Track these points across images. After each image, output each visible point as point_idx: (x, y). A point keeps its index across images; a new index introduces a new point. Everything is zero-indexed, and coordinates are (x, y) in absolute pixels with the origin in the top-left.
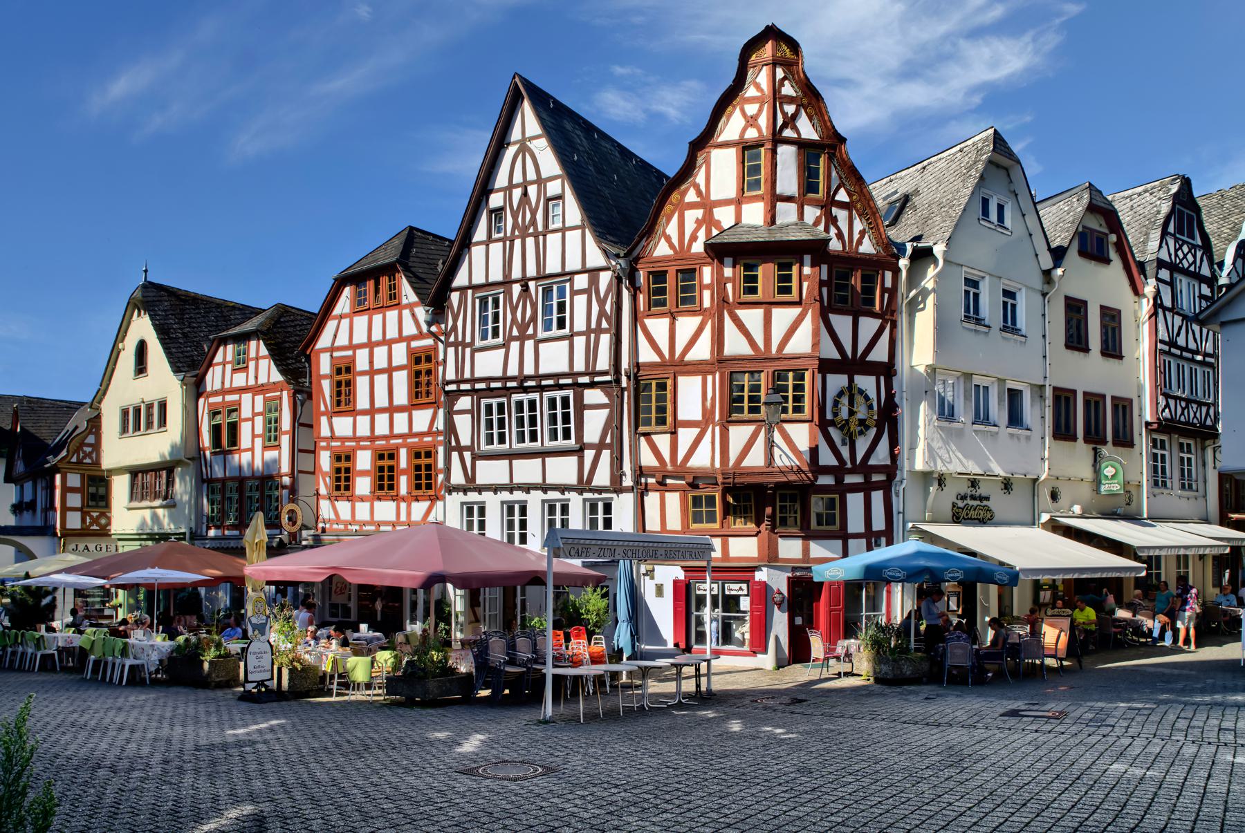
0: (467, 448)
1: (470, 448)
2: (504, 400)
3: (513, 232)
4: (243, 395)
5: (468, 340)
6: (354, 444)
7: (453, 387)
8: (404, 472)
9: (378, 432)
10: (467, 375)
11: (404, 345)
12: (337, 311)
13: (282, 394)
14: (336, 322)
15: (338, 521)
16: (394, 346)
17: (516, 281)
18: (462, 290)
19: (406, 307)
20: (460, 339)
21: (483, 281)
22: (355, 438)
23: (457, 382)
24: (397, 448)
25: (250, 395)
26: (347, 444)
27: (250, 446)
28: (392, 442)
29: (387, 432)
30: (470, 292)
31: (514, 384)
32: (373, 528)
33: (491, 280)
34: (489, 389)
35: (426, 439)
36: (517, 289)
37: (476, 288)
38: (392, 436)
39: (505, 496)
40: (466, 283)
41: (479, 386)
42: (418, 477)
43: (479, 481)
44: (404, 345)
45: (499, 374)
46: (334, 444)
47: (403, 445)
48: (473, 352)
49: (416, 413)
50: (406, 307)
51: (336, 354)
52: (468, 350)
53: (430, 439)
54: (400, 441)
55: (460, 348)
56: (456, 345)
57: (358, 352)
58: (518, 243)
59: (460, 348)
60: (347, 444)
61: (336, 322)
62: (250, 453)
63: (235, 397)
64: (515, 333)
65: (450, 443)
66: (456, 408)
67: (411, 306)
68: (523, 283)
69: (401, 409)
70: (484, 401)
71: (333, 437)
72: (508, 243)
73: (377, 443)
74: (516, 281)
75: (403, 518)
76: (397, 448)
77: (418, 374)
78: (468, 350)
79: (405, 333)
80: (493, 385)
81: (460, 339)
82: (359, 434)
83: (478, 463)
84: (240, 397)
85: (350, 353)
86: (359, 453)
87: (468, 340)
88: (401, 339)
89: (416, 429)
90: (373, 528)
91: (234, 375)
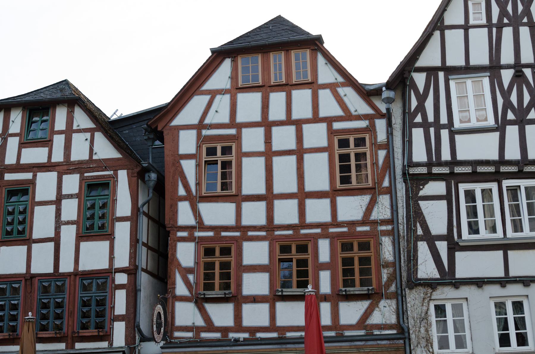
0: (440, 238)
1: (448, 237)
2: (494, 186)
3: (500, 19)
4: (39, 175)
5: (444, 120)
6: (237, 234)
7: (423, 170)
8: (324, 266)
9: (278, 221)
10: (446, 156)
11: (323, 126)
12: (207, 86)
13: (116, 175)
14: (207, 98)
15: (210, 326)
16: (306, 127)
17: (508, 67)
18: (431, 71)
19: (324, 86)
20: (431, 118)
21: (462, 63)
22: (238, 227)
23: (429, 164)
24: (315, 238)
25: (53, 175)
26: (224, 234)
27: (52, 235)
28: (303, 231)
29: (295, 220)
30: (441, 75)
31: (514, 169)
32: (275, 335)
33: (473, 62)
34: (474, 173)
35: (359, 229)
36: (507, 75)
37: (450, 71)
38: (303, 224)
39: (495, 290)
40: (438, 63)
41: (458, 170)
42: (348, 272)
43: (460, 273)
44: (323, 126)
45: (494, 156)
46: (198, 234)
47: (325, 235)
48: (453, 134)
49: (341, 200)
50: (324, 86)
51: (205, 132)
52: (445, 134)
53: (367, 228)
54: (318, 231)
55: (432, 130)
56: (425, 125)
57: (245, 131)
58: (508, 33)
59: (432, 130)
60: (224, 234)
61: (207, 98)
62: (52, 245)
63: (28, 176)
64: (511, 116)
65: (416, 231)
66: (422, 193)
67: (332, 87)
68: (517, 68)
69: (319, 195)
70: (463, 187)
71: (201, 225)
72: (494, 30)
73: (277, 233)
74: (508, 67)
75: (326, 319)
76: (315, 238)
77: (345, 158)
78: (445, 134)
79: (322, 114)
80: (481, 169)
81: (431, 118)
82: (245, 222)
83: (459, 256)
84: (35, 176)
85: (233, 131)
86: (246, 245)
87: (444, 120)
88: (316, 119)
89: (342, 217)
90: (275, 335)
91: (23, 150)
